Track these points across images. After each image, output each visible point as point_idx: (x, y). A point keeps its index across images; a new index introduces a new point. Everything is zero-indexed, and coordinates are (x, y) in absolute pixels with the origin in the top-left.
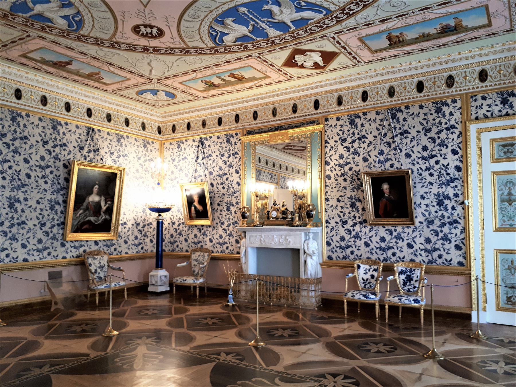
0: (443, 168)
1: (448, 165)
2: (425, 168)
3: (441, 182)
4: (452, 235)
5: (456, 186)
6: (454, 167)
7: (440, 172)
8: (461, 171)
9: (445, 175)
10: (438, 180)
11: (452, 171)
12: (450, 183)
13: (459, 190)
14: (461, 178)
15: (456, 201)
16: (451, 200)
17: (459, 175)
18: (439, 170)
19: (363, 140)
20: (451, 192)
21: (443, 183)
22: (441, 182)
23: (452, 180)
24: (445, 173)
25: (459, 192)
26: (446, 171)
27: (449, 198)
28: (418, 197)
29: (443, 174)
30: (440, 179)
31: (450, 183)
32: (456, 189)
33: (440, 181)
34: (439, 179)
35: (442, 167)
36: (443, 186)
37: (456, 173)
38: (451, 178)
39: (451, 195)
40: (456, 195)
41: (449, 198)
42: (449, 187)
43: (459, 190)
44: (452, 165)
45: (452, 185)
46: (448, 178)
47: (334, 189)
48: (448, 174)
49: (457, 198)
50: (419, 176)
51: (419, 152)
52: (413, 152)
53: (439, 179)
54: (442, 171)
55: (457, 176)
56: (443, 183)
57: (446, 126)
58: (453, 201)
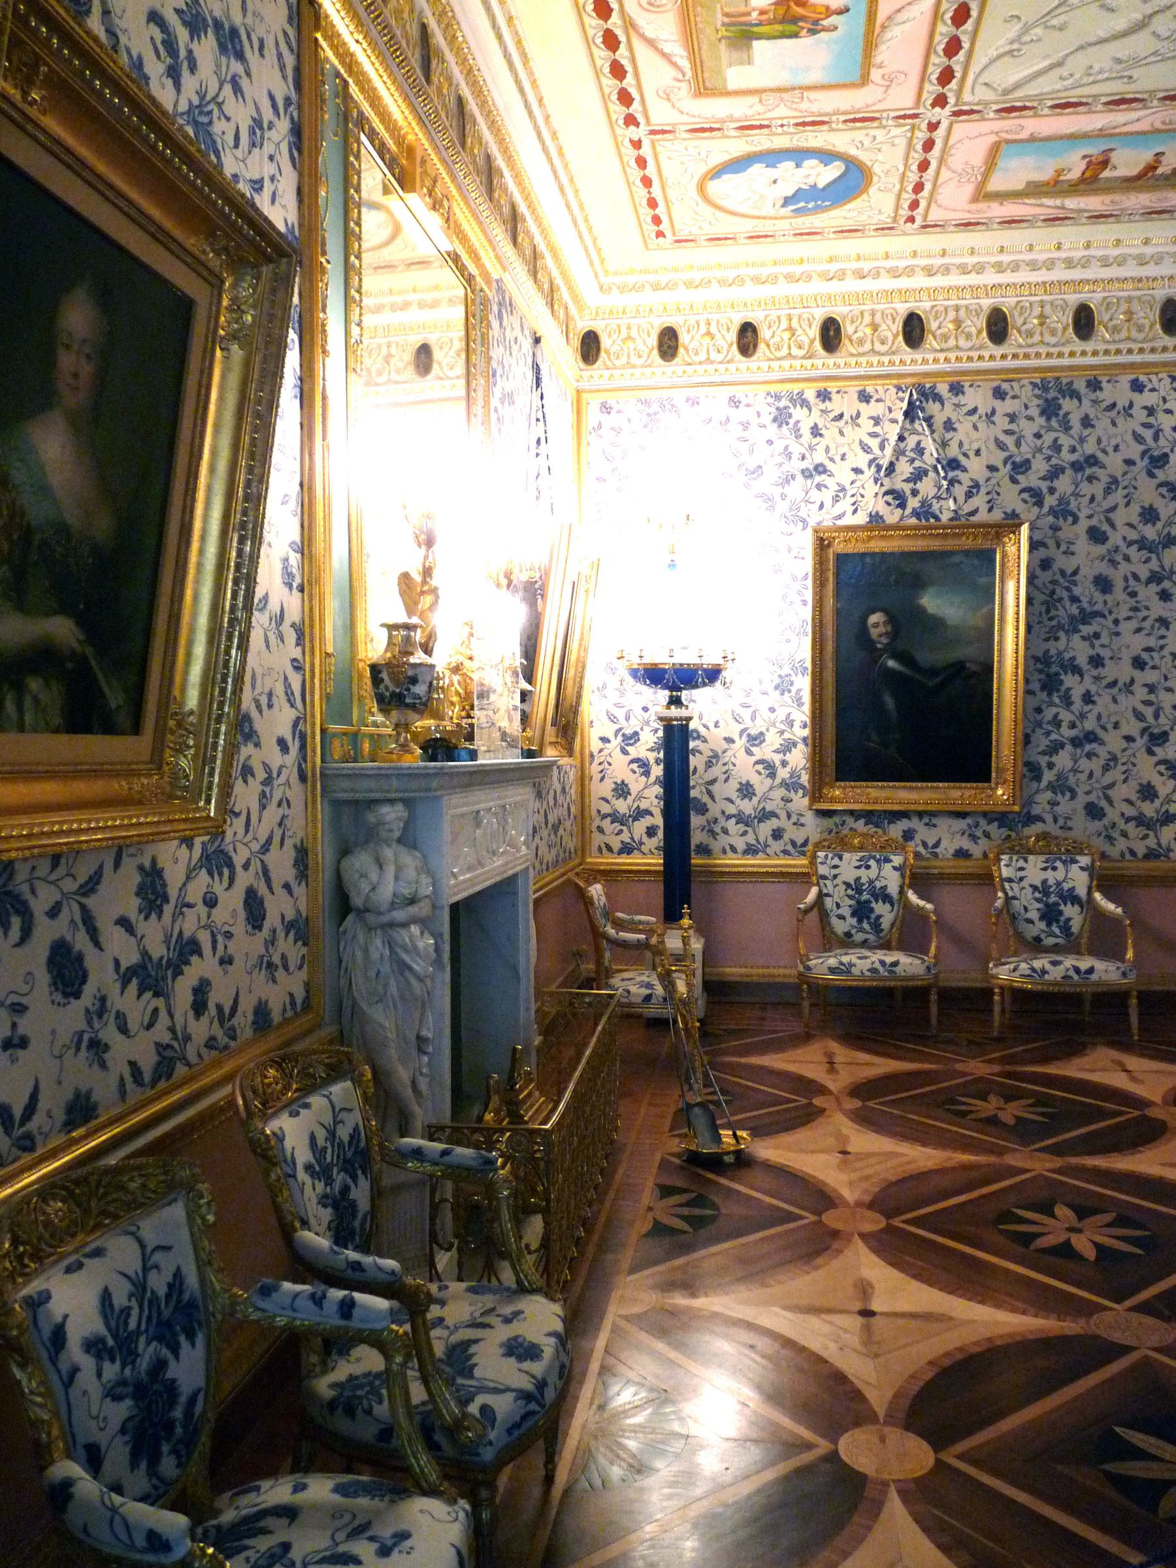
0: (1061, 580)
1: (1075, 573)
2: (1148, 574)
3: (1054, 623)
4: (1079, 775)
5: (1097, 636)
6: (1091, 578)
7: (1053, 593)
8: (1110, 592)
9: (1067, 603)
10: (1045, 617)
11: (1084, 589)
12: (1081, 627)
13: (1103, 646)
14: (1110, 612)
15: (1097, 678)
16: (1082, 676)
17: (1105, 602)
18: (1051, 587)
19: (1088, 471)
20: (1080, 651)
21: (1060, 627)
22: (1054, 623)
23: (1086, 617)
24: (1065, 594)
25: (1105, 653)
26: (1068, 589)
27: (1077, 670)
29: (1060, 600)
30: (1053, 613)
31: (1081, 627)
32: (1097, 643)
33: (1050, 619)
34: (1048, 611)
35: (1058, 577)
36: (1061, 634)
37: (1098, 597)
38: (1082, 610)
39: (1082, 661)
40: (1096, 661)
41: (1077, 670)
42: (1076, 637)
43: (1103, 646)
44: (1088, 572)
45: (1086, 630)
46: (1074, 610)
48: (1075, 599)
49: (1100, 669)
50: (1128, 598)
51: (1131, 525)
52: (1113, 526)
53: (1048, 611)
54: (1058, 590)
55: (1099, 607)
56: (1060, 627)
57: (1073, 457)
58: (1088, 679)
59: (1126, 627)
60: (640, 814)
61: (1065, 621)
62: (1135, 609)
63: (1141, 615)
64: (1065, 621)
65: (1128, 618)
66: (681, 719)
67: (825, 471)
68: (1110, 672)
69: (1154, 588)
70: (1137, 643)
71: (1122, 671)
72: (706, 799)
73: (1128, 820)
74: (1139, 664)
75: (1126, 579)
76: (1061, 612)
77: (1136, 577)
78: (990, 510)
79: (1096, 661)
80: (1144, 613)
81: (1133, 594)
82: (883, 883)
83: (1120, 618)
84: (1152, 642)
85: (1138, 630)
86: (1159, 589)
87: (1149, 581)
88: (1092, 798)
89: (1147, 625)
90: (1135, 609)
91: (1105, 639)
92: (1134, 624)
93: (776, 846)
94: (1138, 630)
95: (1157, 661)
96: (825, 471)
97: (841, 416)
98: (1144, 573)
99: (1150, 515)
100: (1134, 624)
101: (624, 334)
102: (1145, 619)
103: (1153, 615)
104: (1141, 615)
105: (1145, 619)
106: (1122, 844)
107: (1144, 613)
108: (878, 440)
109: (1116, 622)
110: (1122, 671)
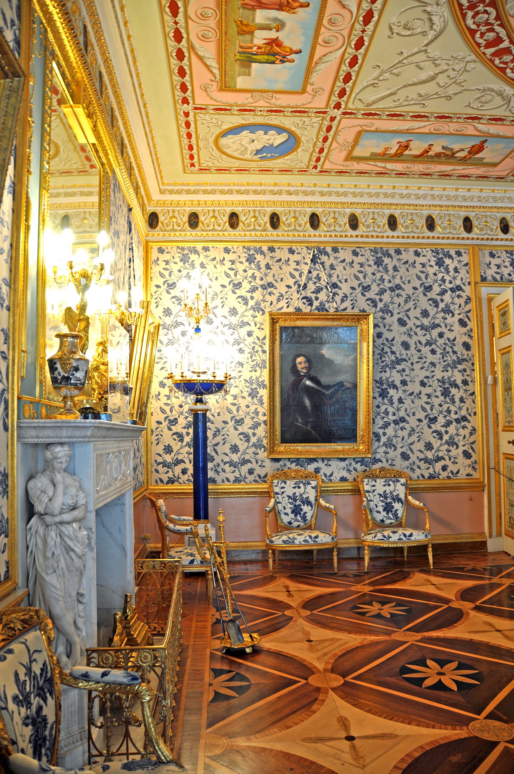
28: (418, 383)
47: (415, 365)
59: (417, 367)
60: (178, 462)
61: (389, 363)
62: (421, 358)
63: (423, 361)
64: (389, 363)
65: (418, 362)
66: (203, 410)
67: (273, 286)
68: (410, 388)
69: (428, 348)
70: (422, 374)
71: (416, 387)
72: (213, 454)
73: (421, 460)
74: (423, 384)
75: (416, 344)
76: (387, 359)
77: (420, 343)
78: (353, 308)
79: (404, 383)
80: (424, 360)
81: (419, 351)
82: (307, 495)
83: (414, 362)
84: (428, 374)
85: (422, 368)
86: (430, 348)
87: (426, 345)
88: (404, 450)
89: (426, 365)
90: (421, 358)
91: (407, 372)
92: (420, 365)
93: (251, 478)
94: (422, 368)
95: (431, 383)
96: (273, 286)
97: (280, 260)
98: (424, 342)
99: (425, 314)
100: (420, 365)
101: (171, 214)
102: (425, 362)
103: (429, 361)
104: (423, 361)
105: (425, 362)
106: (418, 472)
107: (424, 360)
108: (298, 272)
109: (412, 364)
110: (416, 387)
